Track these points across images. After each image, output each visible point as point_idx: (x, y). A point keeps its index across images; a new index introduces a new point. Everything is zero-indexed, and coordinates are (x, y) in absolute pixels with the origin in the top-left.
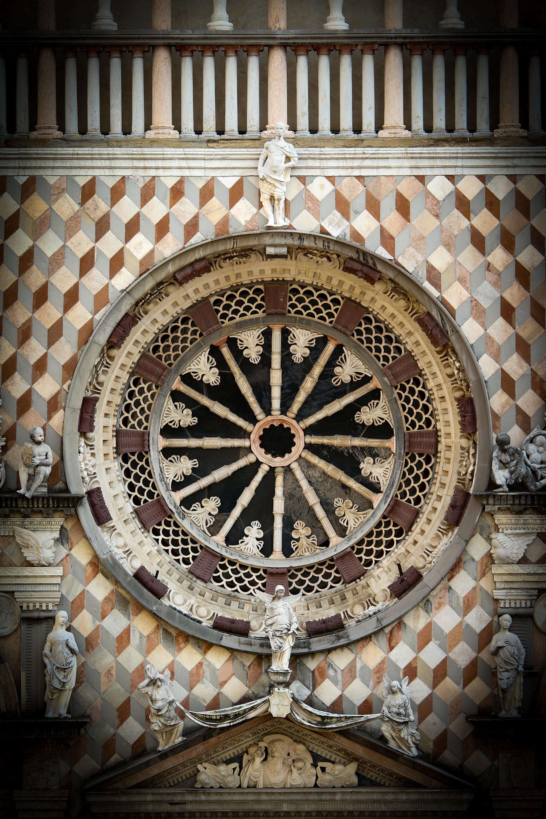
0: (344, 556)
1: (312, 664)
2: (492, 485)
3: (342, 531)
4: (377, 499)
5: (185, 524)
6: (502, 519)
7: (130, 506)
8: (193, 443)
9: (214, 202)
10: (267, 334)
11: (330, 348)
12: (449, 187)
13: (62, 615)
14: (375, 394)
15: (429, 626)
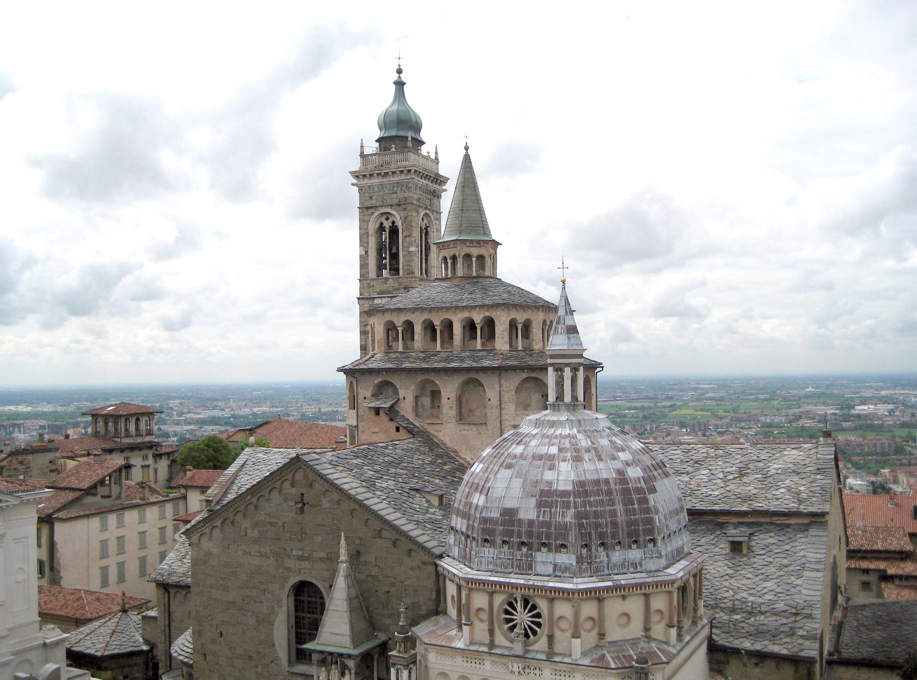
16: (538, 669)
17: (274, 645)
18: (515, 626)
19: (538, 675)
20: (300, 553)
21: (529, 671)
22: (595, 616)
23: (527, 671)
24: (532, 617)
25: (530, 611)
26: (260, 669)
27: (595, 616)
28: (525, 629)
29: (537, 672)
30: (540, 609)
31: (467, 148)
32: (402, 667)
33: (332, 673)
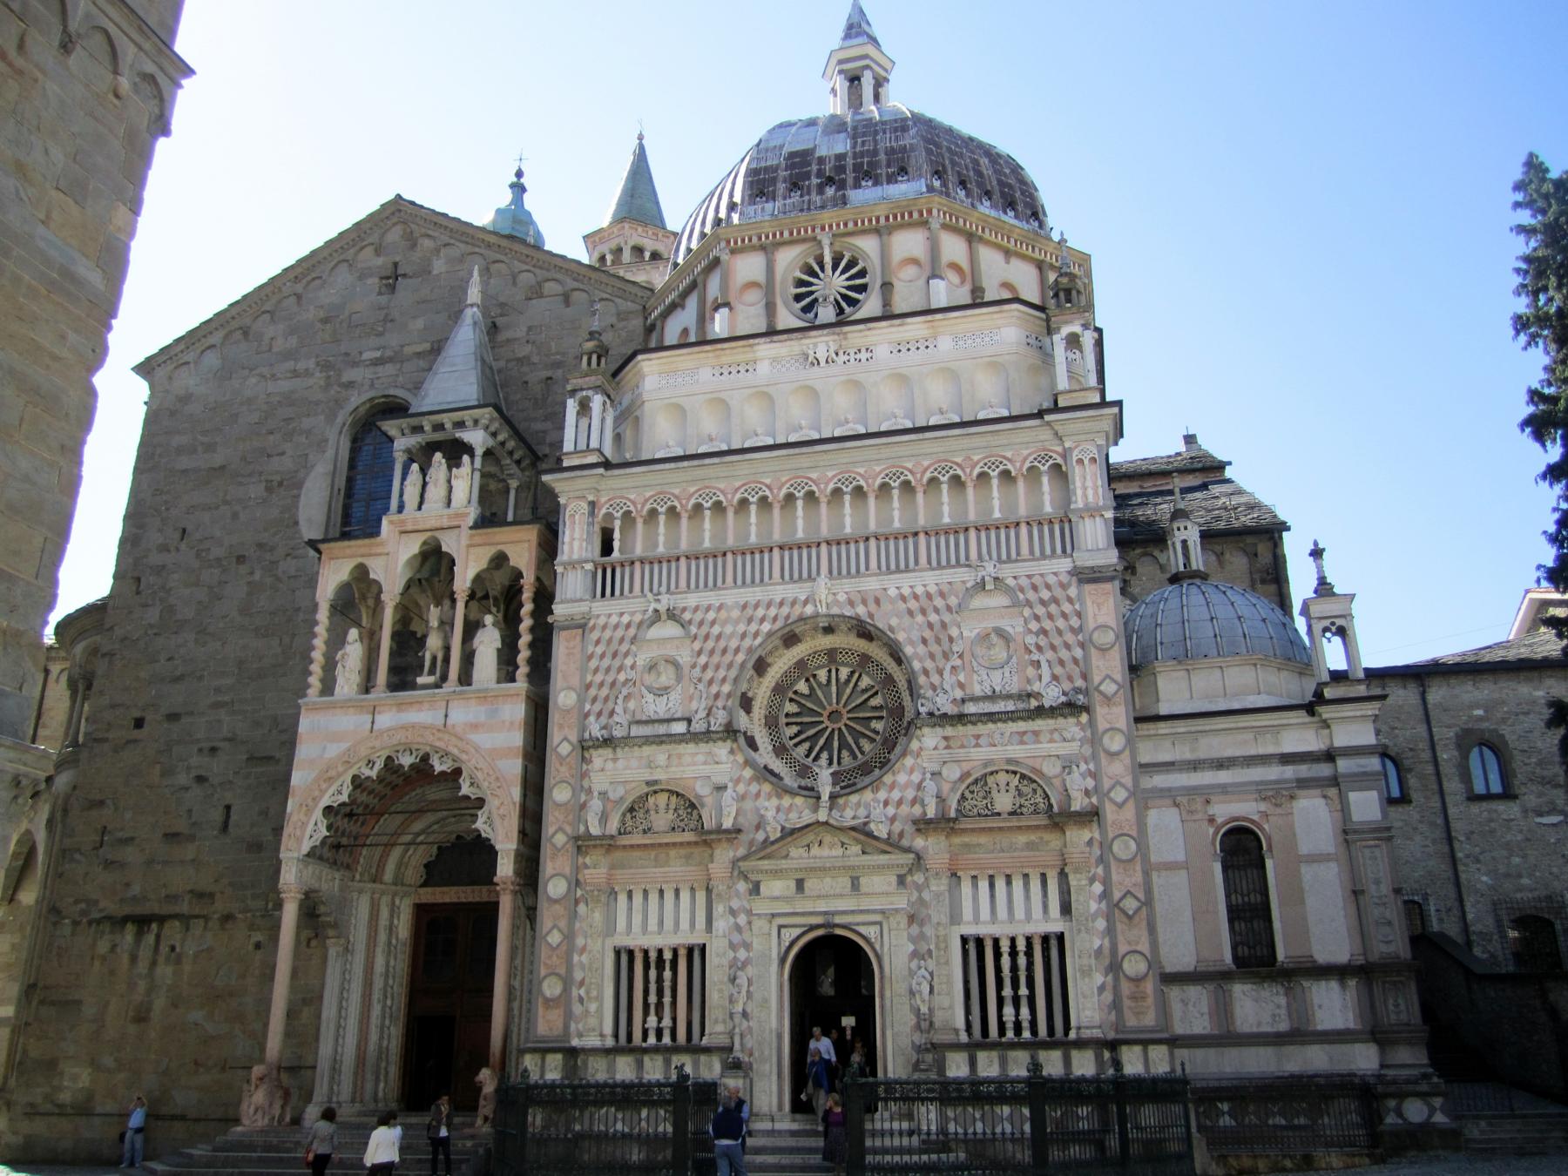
0: (866, 763)
1: (841, 801)
2: (919, 713)
3: (862, 753)
4: (878, 738)
5: (794, 755)
6: (926, 730)
7: (771, 748)
8: (799, 720)
9: (797, 606)
10: (830, 671)
11: (856, 675)
12: (897, 591)
13: (730, 785)
14: (876, 693)
15: (894, 782)
16: (863, 350)
17: (296, 523)
18: (816, 300)
19: (864, 360)
20: (378, 354)
21: (846, 358)
22: (965, 265)
23: (842, 358)
24: (848, 279)
25: (843, 272)
26: (257, 576)
27: (965, 265)
28: (836, 300)
29: (863, 355)
30: (866, 256)
31: (641, 138)
32: (590, 393)
33: (432, 472)
